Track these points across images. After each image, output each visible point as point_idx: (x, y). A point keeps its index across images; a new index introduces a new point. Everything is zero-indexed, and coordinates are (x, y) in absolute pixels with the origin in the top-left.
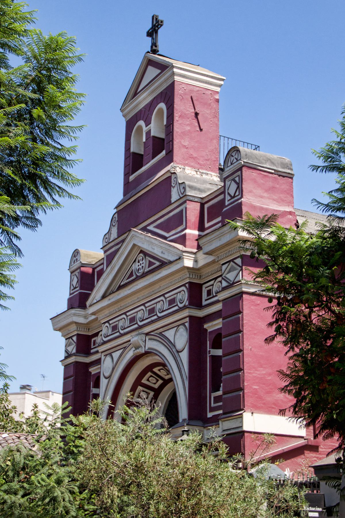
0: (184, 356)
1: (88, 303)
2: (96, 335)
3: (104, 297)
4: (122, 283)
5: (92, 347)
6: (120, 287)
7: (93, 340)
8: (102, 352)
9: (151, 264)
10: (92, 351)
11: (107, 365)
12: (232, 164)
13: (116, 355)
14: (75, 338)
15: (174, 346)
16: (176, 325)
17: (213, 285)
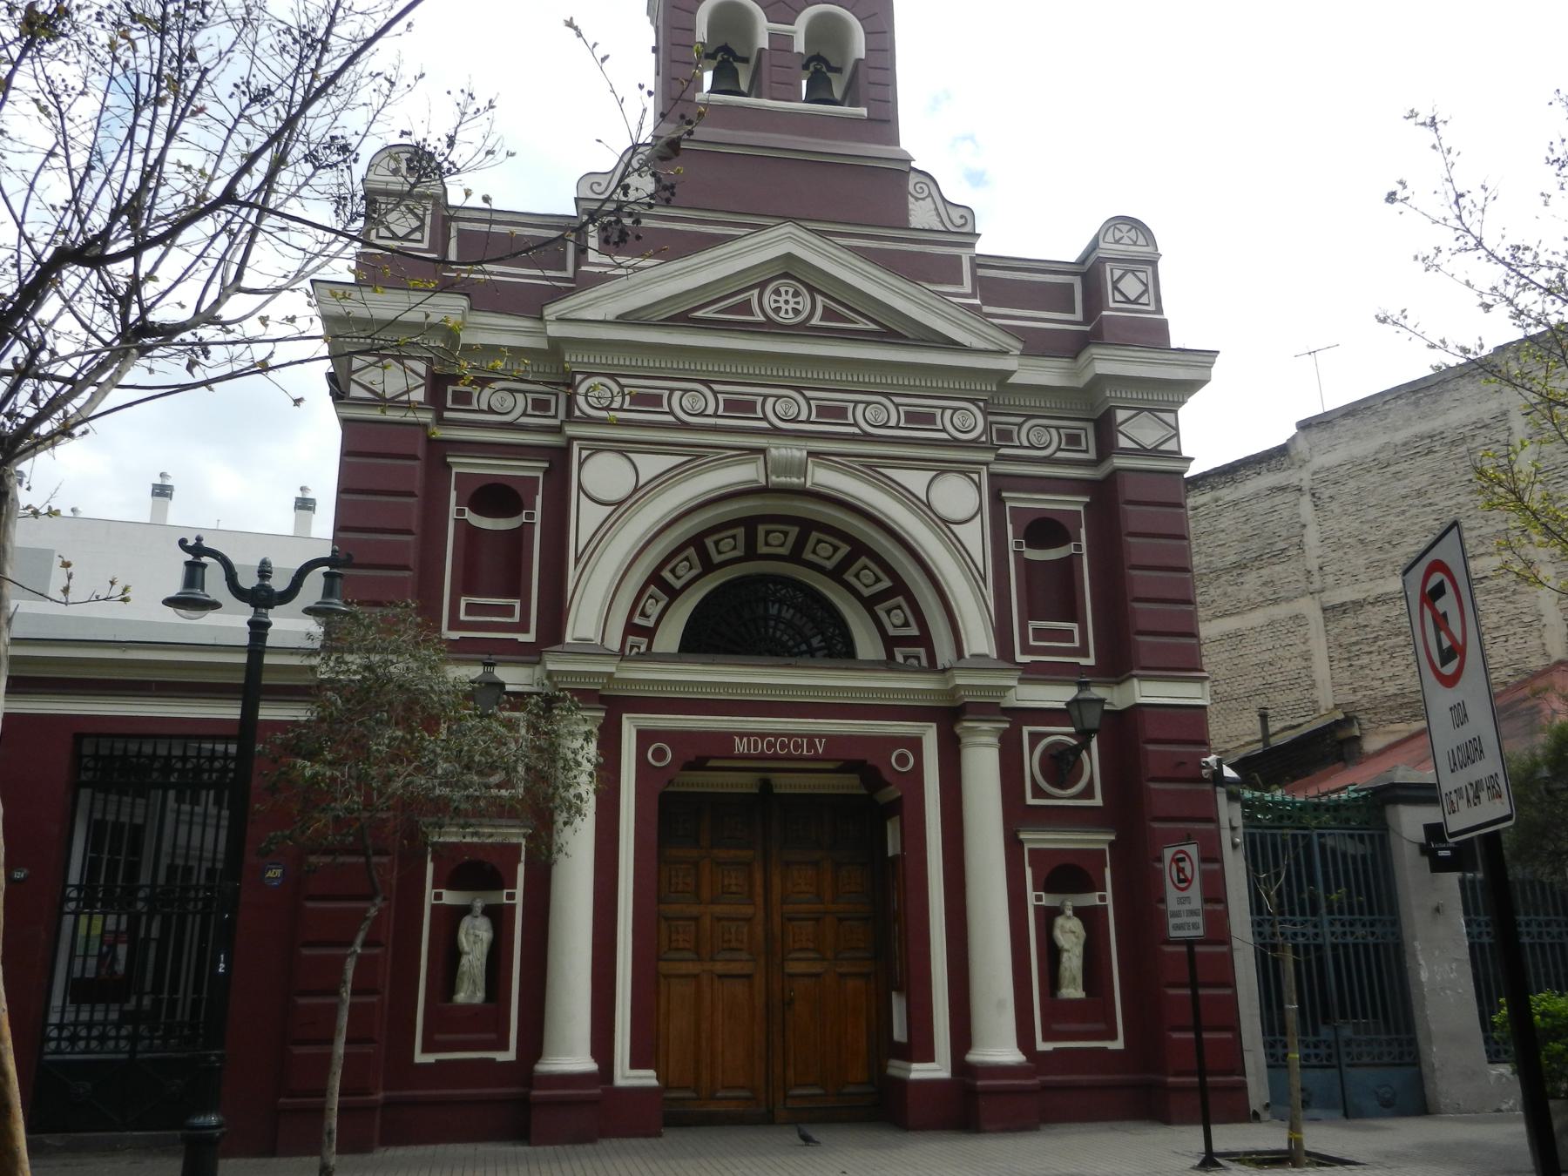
0: (974, 537)
1: (551, 311)
2: (483, 382)
3: (624, 320)
4: (699, 314)
5: (449, 404)
6: (683, 320)
7: (450, 389)
8: (572, 439)
9: (828, 314)
10: (447, 415)
11: (603, 476)
12: (1117, 242)
13: (651, 465)
14: (421, 368)
15: (929, 506)
16: (942, 468)
17: (1020, 426)
